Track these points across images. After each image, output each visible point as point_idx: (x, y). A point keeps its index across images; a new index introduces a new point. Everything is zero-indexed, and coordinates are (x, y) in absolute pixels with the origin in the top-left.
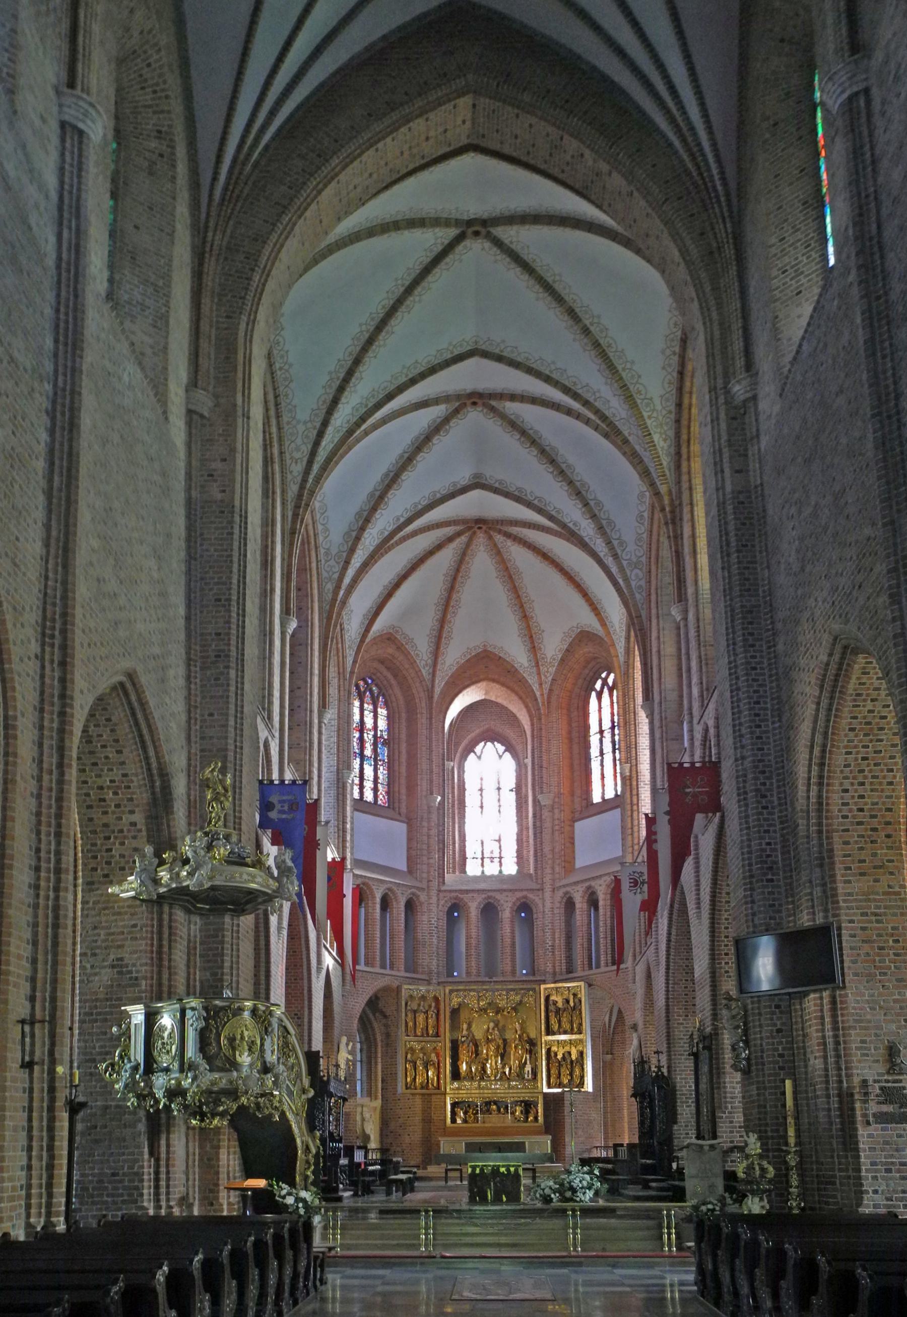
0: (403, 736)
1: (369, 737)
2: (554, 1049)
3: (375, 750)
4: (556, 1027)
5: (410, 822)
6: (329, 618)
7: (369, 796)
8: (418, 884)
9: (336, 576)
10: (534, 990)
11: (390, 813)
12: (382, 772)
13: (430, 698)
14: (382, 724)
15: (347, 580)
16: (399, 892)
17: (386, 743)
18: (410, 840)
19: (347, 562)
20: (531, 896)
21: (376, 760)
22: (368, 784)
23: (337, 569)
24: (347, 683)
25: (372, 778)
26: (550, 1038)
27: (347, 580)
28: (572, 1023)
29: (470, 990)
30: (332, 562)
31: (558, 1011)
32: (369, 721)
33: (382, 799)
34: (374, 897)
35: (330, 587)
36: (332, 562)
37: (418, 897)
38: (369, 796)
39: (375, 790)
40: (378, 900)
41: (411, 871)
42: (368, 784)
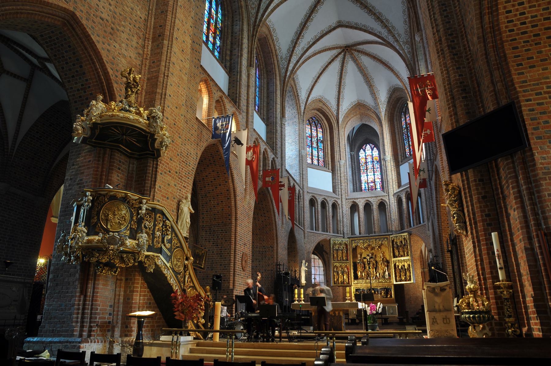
0: (329, 139)
1: (314, 140)
2: (397, 264)
3: (317, 145)
4: (397, 254)
5: (333, 171)
6: (284, 83)
7: (315, 162)
8: (337, 197)
9: (286, 66)
10: (387, 238)
11: (325, 169)
12: (321, 154)
13: (338, 123)
14: (320, 135)
15: (290, 68)
16: (328, 200)
17: (322, 142)
18: (333, 179)
19: (290, 61)
20: (384, 198)
21: (318, 148)
22: (315, 158)
23: (286, 64)
24: (302, 117)
25: (317, 156)
26: (395, 259)
27: (290, 68)
28: (404, 252)
29: (360, 240)
30: (284, 61)
31: (398, 247)
32: (314, 134)
33: (321, 163)
34: (317, 202)
35: (284, 71)
36: (284, 61)
37: (337, 202)
38: (315, 162)
39: (318, 160)
40: (319, 203)
41: (334, 191)
42: (315, 158)
